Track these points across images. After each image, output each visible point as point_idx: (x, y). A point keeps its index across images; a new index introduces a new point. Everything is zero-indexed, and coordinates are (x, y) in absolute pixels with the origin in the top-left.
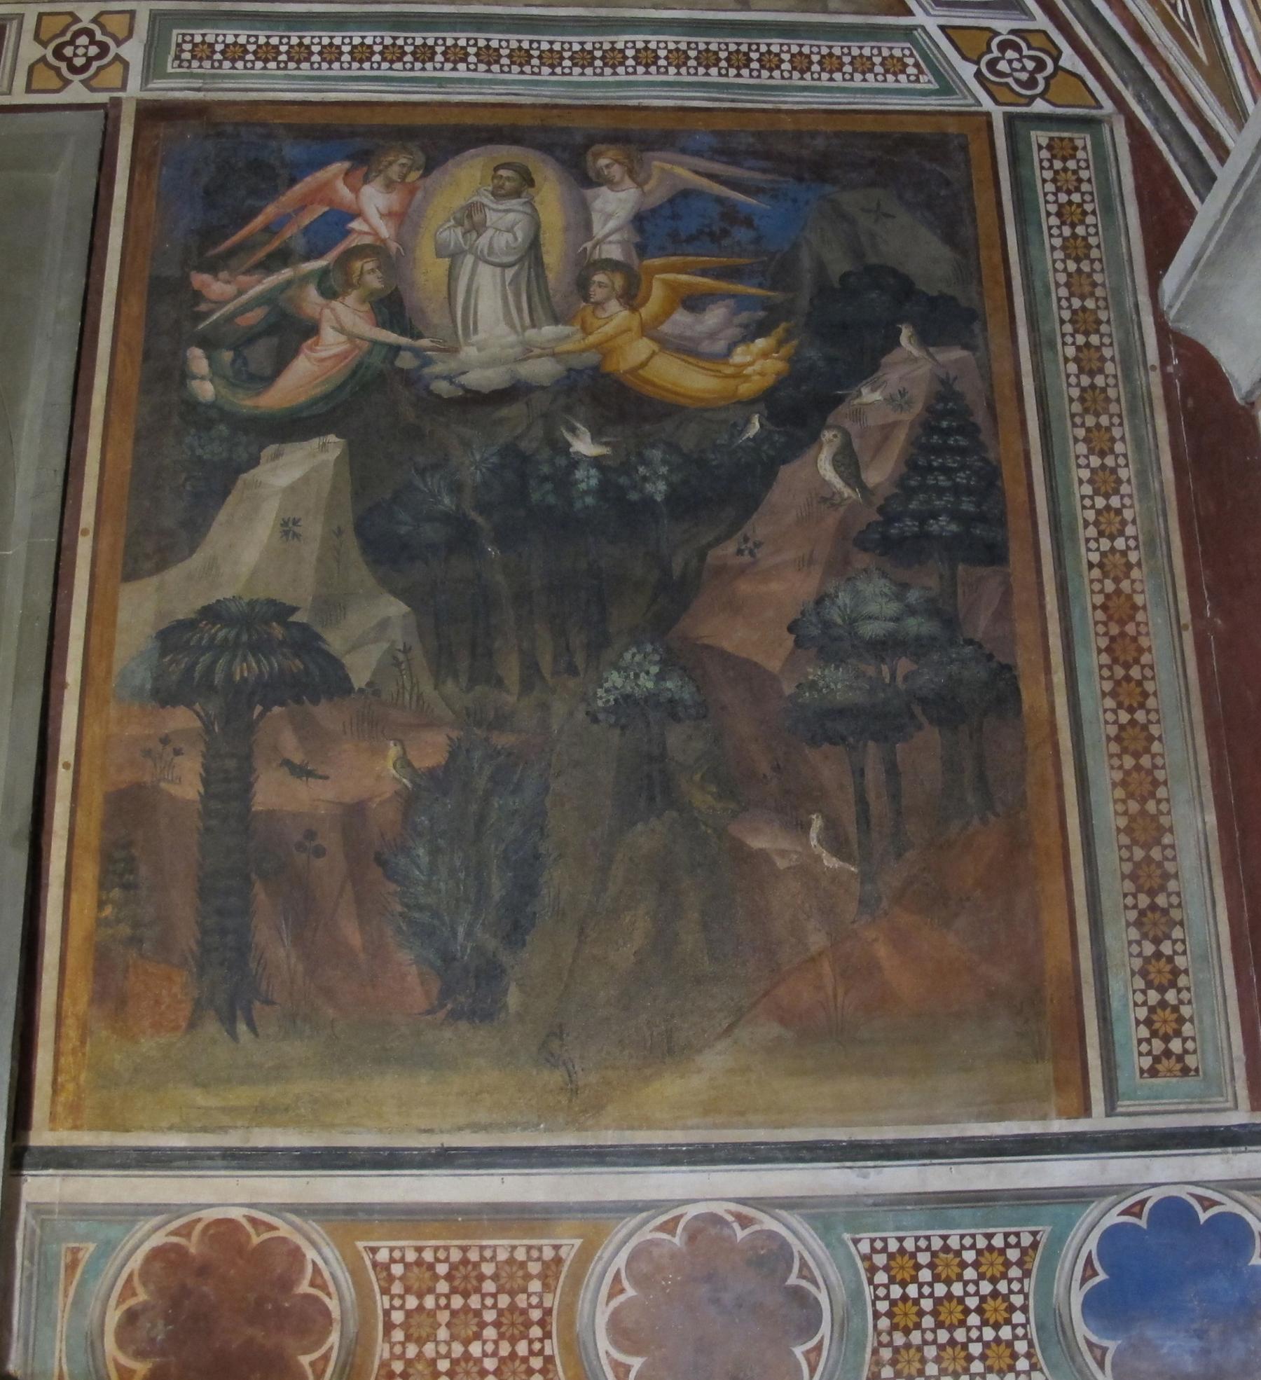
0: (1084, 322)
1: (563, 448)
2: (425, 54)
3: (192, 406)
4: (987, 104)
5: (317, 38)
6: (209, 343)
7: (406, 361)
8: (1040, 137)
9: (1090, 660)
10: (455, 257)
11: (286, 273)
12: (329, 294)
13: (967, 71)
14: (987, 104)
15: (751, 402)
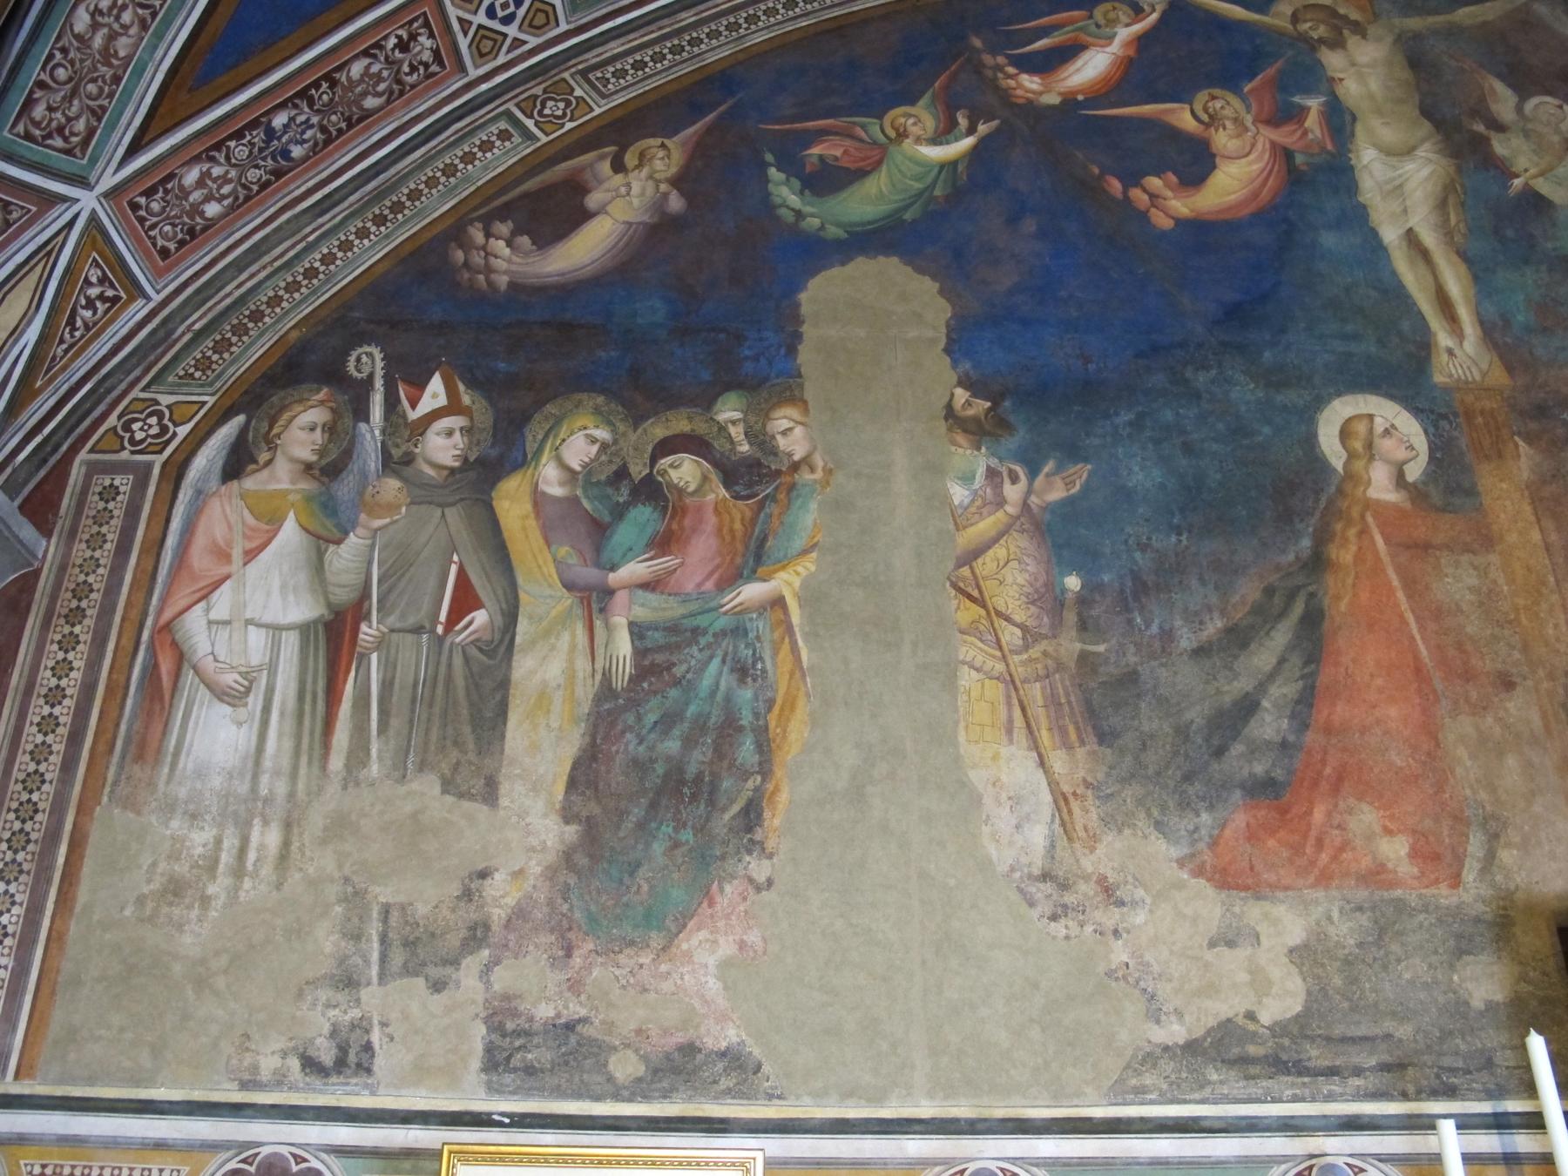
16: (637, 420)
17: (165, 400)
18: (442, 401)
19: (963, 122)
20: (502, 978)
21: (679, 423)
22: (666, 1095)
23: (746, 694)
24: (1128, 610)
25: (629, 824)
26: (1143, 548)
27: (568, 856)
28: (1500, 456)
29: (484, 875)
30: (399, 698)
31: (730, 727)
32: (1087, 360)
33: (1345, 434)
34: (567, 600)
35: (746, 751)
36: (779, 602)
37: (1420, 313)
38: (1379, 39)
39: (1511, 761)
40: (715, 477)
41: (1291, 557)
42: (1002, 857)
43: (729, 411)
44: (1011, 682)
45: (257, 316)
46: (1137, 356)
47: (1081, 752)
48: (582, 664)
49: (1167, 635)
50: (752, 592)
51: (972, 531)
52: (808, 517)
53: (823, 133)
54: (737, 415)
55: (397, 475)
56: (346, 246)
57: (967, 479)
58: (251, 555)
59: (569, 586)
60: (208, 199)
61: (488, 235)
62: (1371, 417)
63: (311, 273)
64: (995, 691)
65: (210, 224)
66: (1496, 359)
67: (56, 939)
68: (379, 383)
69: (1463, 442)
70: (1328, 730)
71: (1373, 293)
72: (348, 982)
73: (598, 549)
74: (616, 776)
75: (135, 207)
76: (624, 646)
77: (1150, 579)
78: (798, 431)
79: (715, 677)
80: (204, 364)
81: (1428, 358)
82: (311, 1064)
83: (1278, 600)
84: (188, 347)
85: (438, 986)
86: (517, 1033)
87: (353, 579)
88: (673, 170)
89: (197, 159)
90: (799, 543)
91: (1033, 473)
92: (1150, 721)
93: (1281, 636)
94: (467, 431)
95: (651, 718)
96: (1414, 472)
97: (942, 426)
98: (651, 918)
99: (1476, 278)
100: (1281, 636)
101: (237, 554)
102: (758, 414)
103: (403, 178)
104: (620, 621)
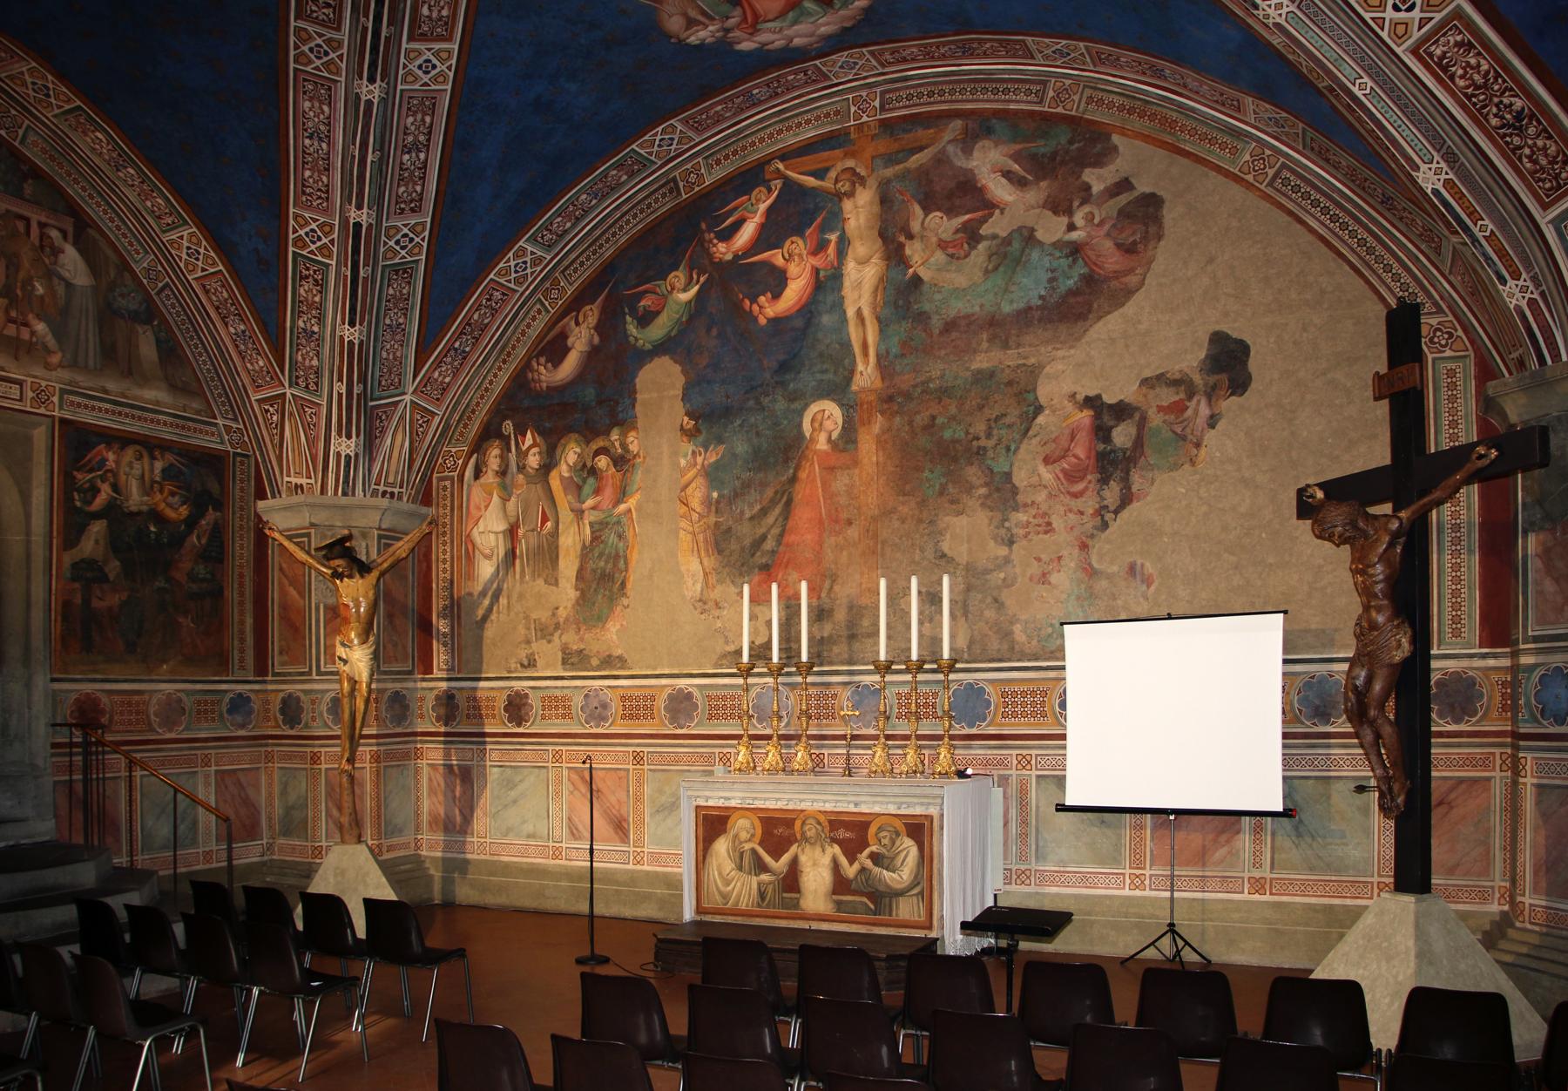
0: (242, 509)
1: (148, 528)
2: (120, 414)
3: (75, 507)
4: (229, 449)
5: (97, 404)
6: (79, 491)
7: (118, 502)
8: (239, 459)
9: (236, 586)
10: (127, 475)
11: (93, 475)
12: (103, 482)
13: (226, 437)
14: (229, 449)
15: (181, 521)
16: (588, 443)
17: (454, 450)
18: (531, 442)
19: (695, 277)
20: (564, 638)
21: (600, 443)
22: (604, 669)
23: (621, 544)
24: (731, 504)
25: (592, 590)
26: (738, 478)
27: (577, 602)
28: (869, 423)
29: (557, 608)
30: (531, 557)
31: (617, 556)
32: (728, 397)
33: (813, 420)
34: (571, 516)
35: (621, 564)
36: (629, 511)
37: (854, 354)
38: (871, 188)
39: (845, 553)
40: (611, 463)
41: (785, 477)
42: (688, 594)
43: (615, 435)
44: (694, 534)
45: (473, 412)
46: (745, 393)
47: (712, 558)
48: (577, 538)
49: (742, 513)
50: (622, 507)
51: (686, 477)
52: (638, 477)
53: (646, 292)
54: (617, 437)
55: (522, 473)
56: (495, 376)
57: (685, 456)
58: (487, 507)
59: (572, 510)
60: (445, 377)
61: (538, 364)
62: (824, 410)
63: (487, 390)
64: (689, 537)
65: (449, 384)
66: (879, 375)
67: (459, 635)
68: (512, 436)
69: (856, 418)
70: (788, 545)
71: (837, 346)
72: (528, 642)
73: (579, 496)
74: (588, 575)
75: (422, 392)
76: (588, 531)
77: (739, 491)
78: (636, 442)
79: (613, 539)
80: (462, 434)
81: (851, 378)
82: (522, 665)
83: (779, 496)
84: (456, 427)
85: (549, 642)
86: (569, 654)
87: (514, 514)
88: (595, 321)
89: (436, 369)
90: (635, 487)
91: (706, 451)
92: (734, 546)
93: (778, 510)
94: (540, 453)
95: (596, 555)
96: (835, 435)
97: (679, 433)
98: (599, 618)
99: (881, 331)
100: (778, 510)
101: (483, 507)
102: (624, 435)
103: (509, 339)
104: (587, 522)
